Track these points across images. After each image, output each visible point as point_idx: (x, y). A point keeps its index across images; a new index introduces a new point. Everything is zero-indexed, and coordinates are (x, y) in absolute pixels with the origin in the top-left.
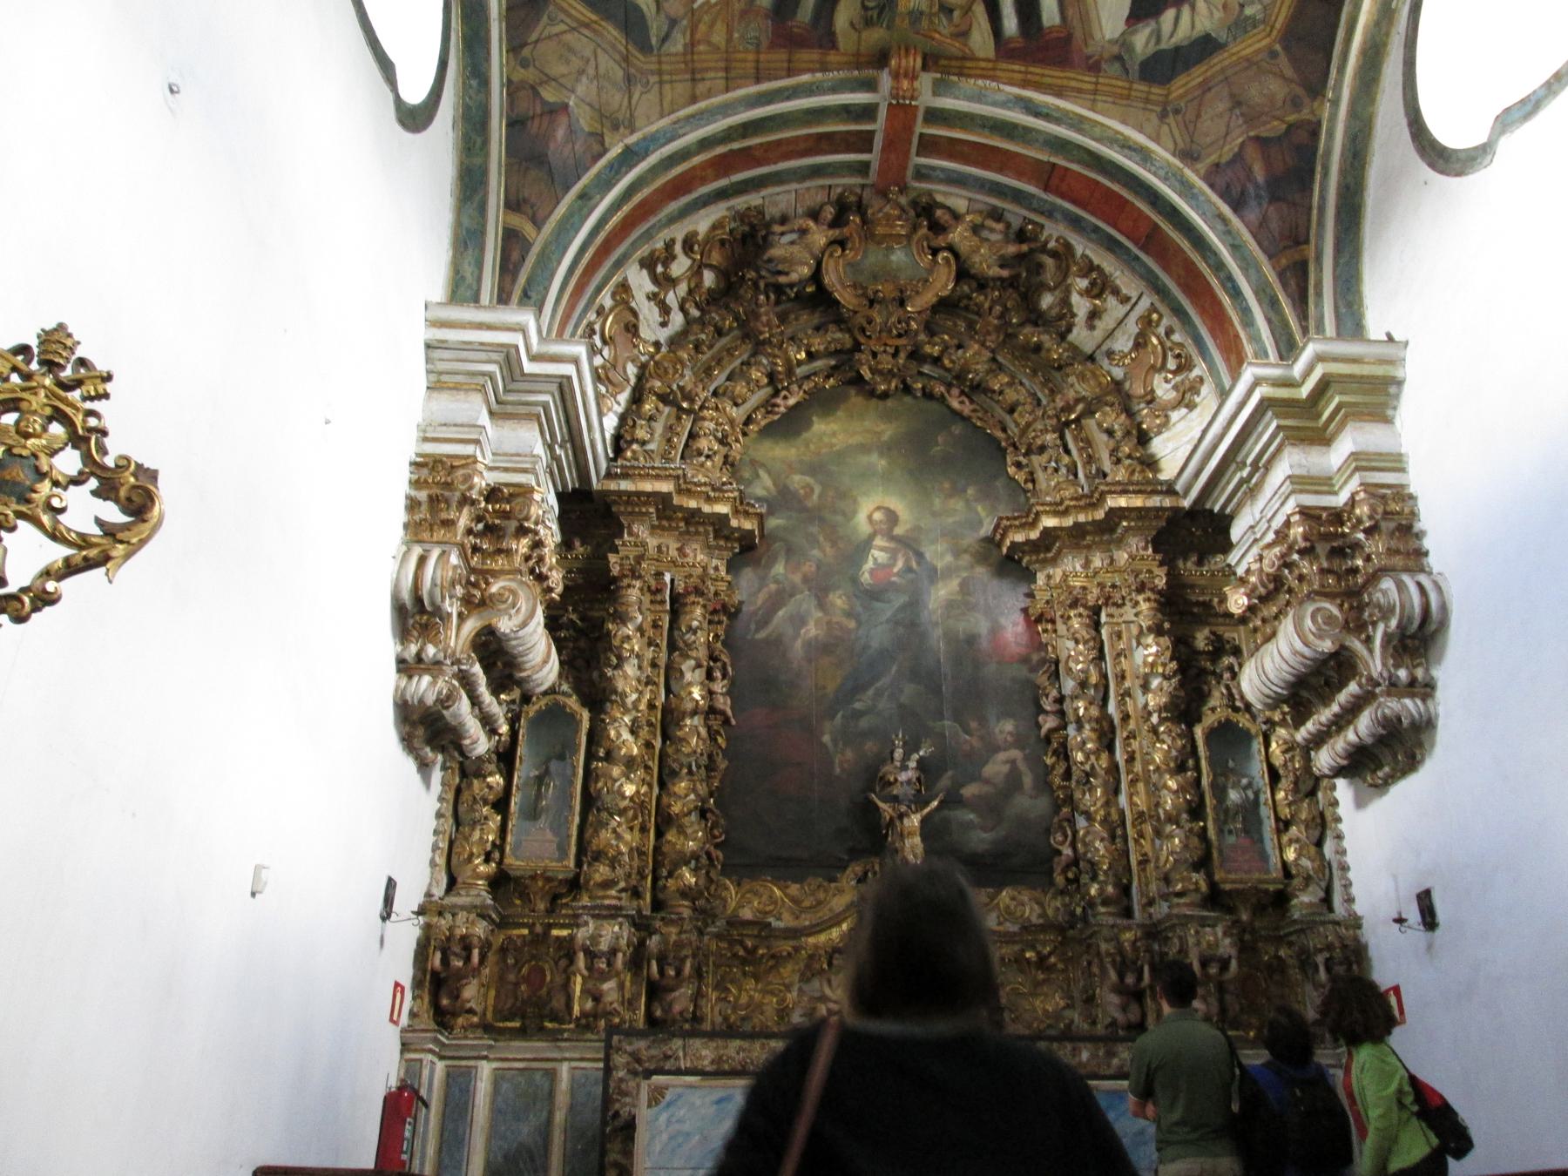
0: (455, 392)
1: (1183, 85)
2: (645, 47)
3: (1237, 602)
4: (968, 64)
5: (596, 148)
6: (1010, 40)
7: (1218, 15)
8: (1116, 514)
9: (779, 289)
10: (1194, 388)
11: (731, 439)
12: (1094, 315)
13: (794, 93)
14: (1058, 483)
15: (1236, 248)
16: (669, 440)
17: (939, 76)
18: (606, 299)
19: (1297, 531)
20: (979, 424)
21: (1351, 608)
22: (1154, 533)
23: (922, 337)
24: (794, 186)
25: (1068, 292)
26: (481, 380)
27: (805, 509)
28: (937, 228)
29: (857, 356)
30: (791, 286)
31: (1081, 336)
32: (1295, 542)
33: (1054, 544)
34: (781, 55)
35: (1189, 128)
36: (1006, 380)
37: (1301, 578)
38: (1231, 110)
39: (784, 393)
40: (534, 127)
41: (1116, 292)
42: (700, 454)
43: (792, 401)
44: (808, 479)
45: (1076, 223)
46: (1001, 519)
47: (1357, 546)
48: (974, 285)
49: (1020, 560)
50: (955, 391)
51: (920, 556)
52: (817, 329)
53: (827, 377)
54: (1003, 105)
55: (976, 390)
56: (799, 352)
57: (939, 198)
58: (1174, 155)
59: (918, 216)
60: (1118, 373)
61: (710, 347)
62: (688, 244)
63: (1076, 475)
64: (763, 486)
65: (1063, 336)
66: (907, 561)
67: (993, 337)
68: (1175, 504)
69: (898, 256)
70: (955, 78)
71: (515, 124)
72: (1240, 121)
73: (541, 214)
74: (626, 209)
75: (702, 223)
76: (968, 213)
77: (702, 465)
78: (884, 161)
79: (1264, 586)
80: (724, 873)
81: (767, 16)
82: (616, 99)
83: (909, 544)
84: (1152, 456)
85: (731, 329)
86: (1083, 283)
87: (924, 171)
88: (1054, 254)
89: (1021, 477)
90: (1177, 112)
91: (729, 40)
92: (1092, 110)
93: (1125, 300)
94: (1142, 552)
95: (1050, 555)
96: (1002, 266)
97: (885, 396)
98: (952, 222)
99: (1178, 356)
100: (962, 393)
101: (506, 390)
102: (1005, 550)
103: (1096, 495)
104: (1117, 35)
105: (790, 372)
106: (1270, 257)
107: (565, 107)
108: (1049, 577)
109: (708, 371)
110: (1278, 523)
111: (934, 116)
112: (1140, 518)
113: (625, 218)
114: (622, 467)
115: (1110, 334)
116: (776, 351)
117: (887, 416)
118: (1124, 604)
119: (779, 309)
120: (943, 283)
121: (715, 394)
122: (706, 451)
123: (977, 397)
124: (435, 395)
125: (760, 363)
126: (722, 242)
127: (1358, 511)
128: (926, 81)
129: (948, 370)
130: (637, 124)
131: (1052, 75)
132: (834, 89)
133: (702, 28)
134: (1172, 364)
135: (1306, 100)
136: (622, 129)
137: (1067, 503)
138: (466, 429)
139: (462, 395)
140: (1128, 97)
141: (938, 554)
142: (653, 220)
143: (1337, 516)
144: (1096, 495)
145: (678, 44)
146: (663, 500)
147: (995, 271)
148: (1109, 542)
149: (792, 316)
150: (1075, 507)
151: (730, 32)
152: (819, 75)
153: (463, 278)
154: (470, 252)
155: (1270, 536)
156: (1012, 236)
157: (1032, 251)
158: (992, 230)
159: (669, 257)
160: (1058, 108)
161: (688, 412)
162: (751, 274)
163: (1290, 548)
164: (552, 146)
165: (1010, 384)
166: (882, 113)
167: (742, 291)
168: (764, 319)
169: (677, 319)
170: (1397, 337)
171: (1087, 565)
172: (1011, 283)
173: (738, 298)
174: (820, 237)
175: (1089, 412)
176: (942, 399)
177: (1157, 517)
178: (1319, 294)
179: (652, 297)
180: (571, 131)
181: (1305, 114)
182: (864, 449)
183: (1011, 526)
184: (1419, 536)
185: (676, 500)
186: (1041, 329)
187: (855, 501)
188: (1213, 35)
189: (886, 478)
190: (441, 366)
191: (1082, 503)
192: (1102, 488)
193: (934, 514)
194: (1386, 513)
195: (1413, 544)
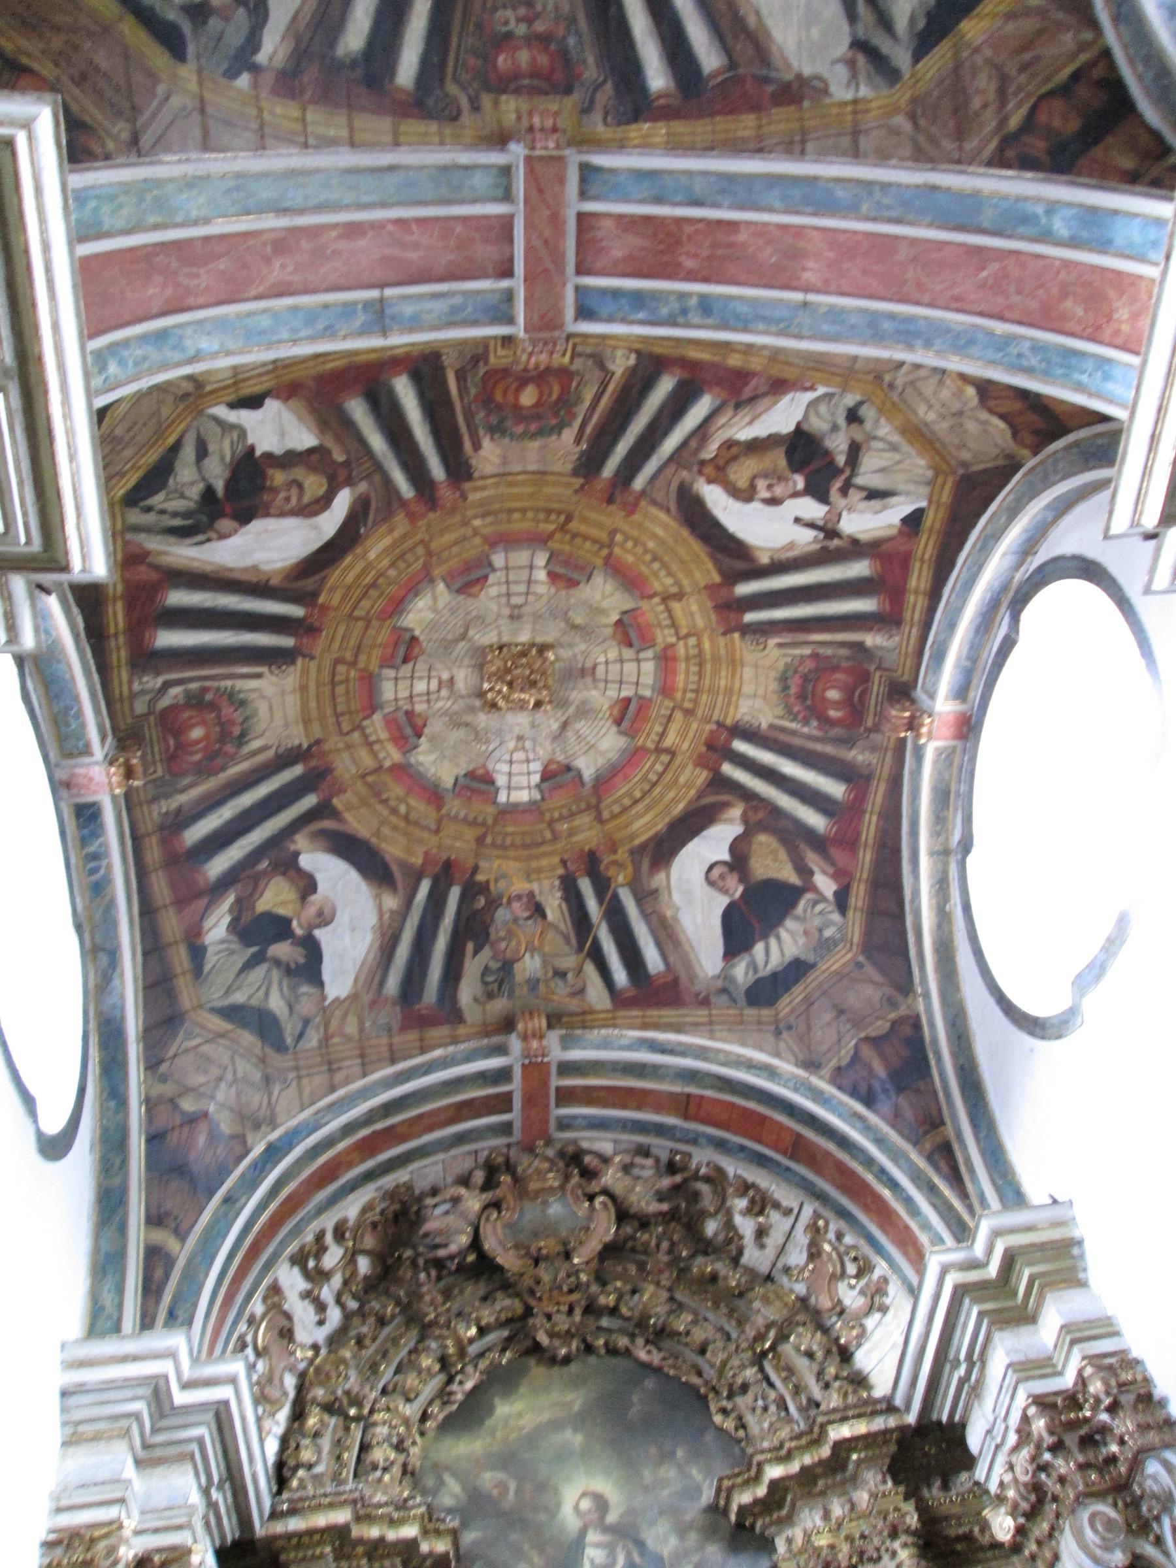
0: (94, 1444)
1: (788, 1004)
2: (280, 1047)
3: (1003, 1526)
4: (589, 1017)
5: (239, 1149)
6: (622, 991)
7: (802, 940)
8: (843, 1447)
9: (439, 1264)
10: (880, 1289)
11: (408, 1443)
12: (761, 1233)
13: (429, 1068)
14: (771, 1425)
15: (880, 1141)
16: (339, 1457)
17: (564, 1032)
18: (257, 1306)
19: (1039, 1425)
20: (672, 1372)
21: (1126, 1505)
22: (887, 1461)
23: (594, 1288)
24: (440, 1156)
25: (729, 1214)
26: (124, 1423)
27: (501, 1514)
28: (588, 1174)
29: (531, 1321)
30: (451, 1257)
31: (753, 1257)
32: (1041, 1439)
33: (784, 1499)
34: (412, 1036)
35: (805, 1040)
36: (690, 1318)
37: (1062, 1480)
38: (837, 1017)
39: (458, 1378)
40: (173, 1139)
41: (777, 1205)
42: (375, 1467)
43: (469, 1385)
44: (500, 1475)
45: (721, 1145)
46: (721, 1480)
47: (1104, 1429)
48: (636, 1223)
49: (753, 1527)
50: (640, 1341)
51: (641, 1545)
52: (484, 1299)
53: (503, 1350)
54: (629, 1048)
55: (660, 1335)
56: (468, 1328)
57: (585, 1145)
58: (797, 1065)
59: (568, 1165)
60: (800, 1289)
61: (374, 1339)
62: (339, 1233)
63: (786, 1409)
64: (452, 1493)
65: (736, 1261)
66: (629, 1554)
67: (666, 1274)
68: (899, 1423)
69: (555, 1209)
70: (579, 1032)
71: (154, 1139)
72: (849, 1026)
73: (185, 1226)
74: (273, 1206)
75: (351, 1209)
76: (615, 1154)
77: (380, 1480)
78: (526, 1119)
79: (1026, 1499)
81: (394, 1004)
82: (256, 1099)
84: (859, 1373)
85: (393, 1316)
86: (742, 1203)
87: (565, 1121)
88: (707, 1180)
89: (729, 1424)
90: (789, 1028)
91: (361, 1030)
92: (712, 1038)
93: (788, 1212)
94: (882, 1488)
95: (784, 1512)
96: (661, 1200)
97: (567, 1360)
98: (602, 1166)
99: (855, 1259)
100: (647, 1342)
101: (155, 1430)
102: (733, 1517)
103: (816, 1429)
104: (718, 971)
105: (462, 1352)
106: (915, 1143)
107: (205, 1115)
108: (789, 1541)
109: (374, 1367)
110: (1015, 1419)
111: (566, 1068)
112: (867, 1447)
113: (272, 1217)
114: (290, 1501)
115: (782, 1250)
116: (445, 1332)
117: (575, 1383)
118: (879, 1558)
119: (441, 1284)
120: (605, 1229)
121: (384, 1392)
122: (381, 1464)
123: (666, 1343)
124: (71, 1450)
125: (427, 1349)
126: (374, 1225)
127: (1092, 1389)
128: (553, 1039)
129: (628, 1319)
130: (279, 1121)
131: (668, 1014)
132: (468, 1059)
133: (334, 1023)
134: (851, 1269)
135: (900, 998)
136: (263, 1128)
137: (787, 1445)
138: (108, 1487)
139: (102, 1445)
140: (742, 1023)
142: (301, 1214)
143: (1073, 1400)
144: (816, 1429)
145: (313, 1039)
146: (339, 1534)
147: (654, 1207)
148: (844, 1482)
149: (456, 1291)
150: (798, 1448)
151: (361, 1023)
152: (451, 1049)
153: (102, 1308)
154: (109, 1277)
155: (1012, 1438)
156: (663, 1169)
157: (685, 1181)
158: (643, 1167)
159: (320, 1248)
160: (680, 1044)
161: (357, 1419)
162: (408, 1253)
163: (1038, 1447)
164: (193, 1156)
165: (695, 1322)
166: (517, 1073)
167: (401, 1273)
168: (427, 1298)
169: (334, 1316)
170: (1060, 1199)
171: (826, 1516)
172: (671, 1216)
173: (397, 1281)
174: (473, 1203)
175: (783, 1337)
176: (627, 1353)
177: (886, 1442)
178: (971, 1170)
179: (306, 1295)
180: (213, 1137)
181: (903, 1011)
182: (556, 1425)
183: (733, 1486)
184: (1162, 1403)
185: (356, 1532)
186: (712, 1257)
187: (556, 1492)
188: (803, 957)
189: (586, 1454)
190: (78, 1415)
191: (803, 1441)
192: (820, 1419)
193: (646, 1489)
194: (1121, 1385)
195: (1160, 1416)
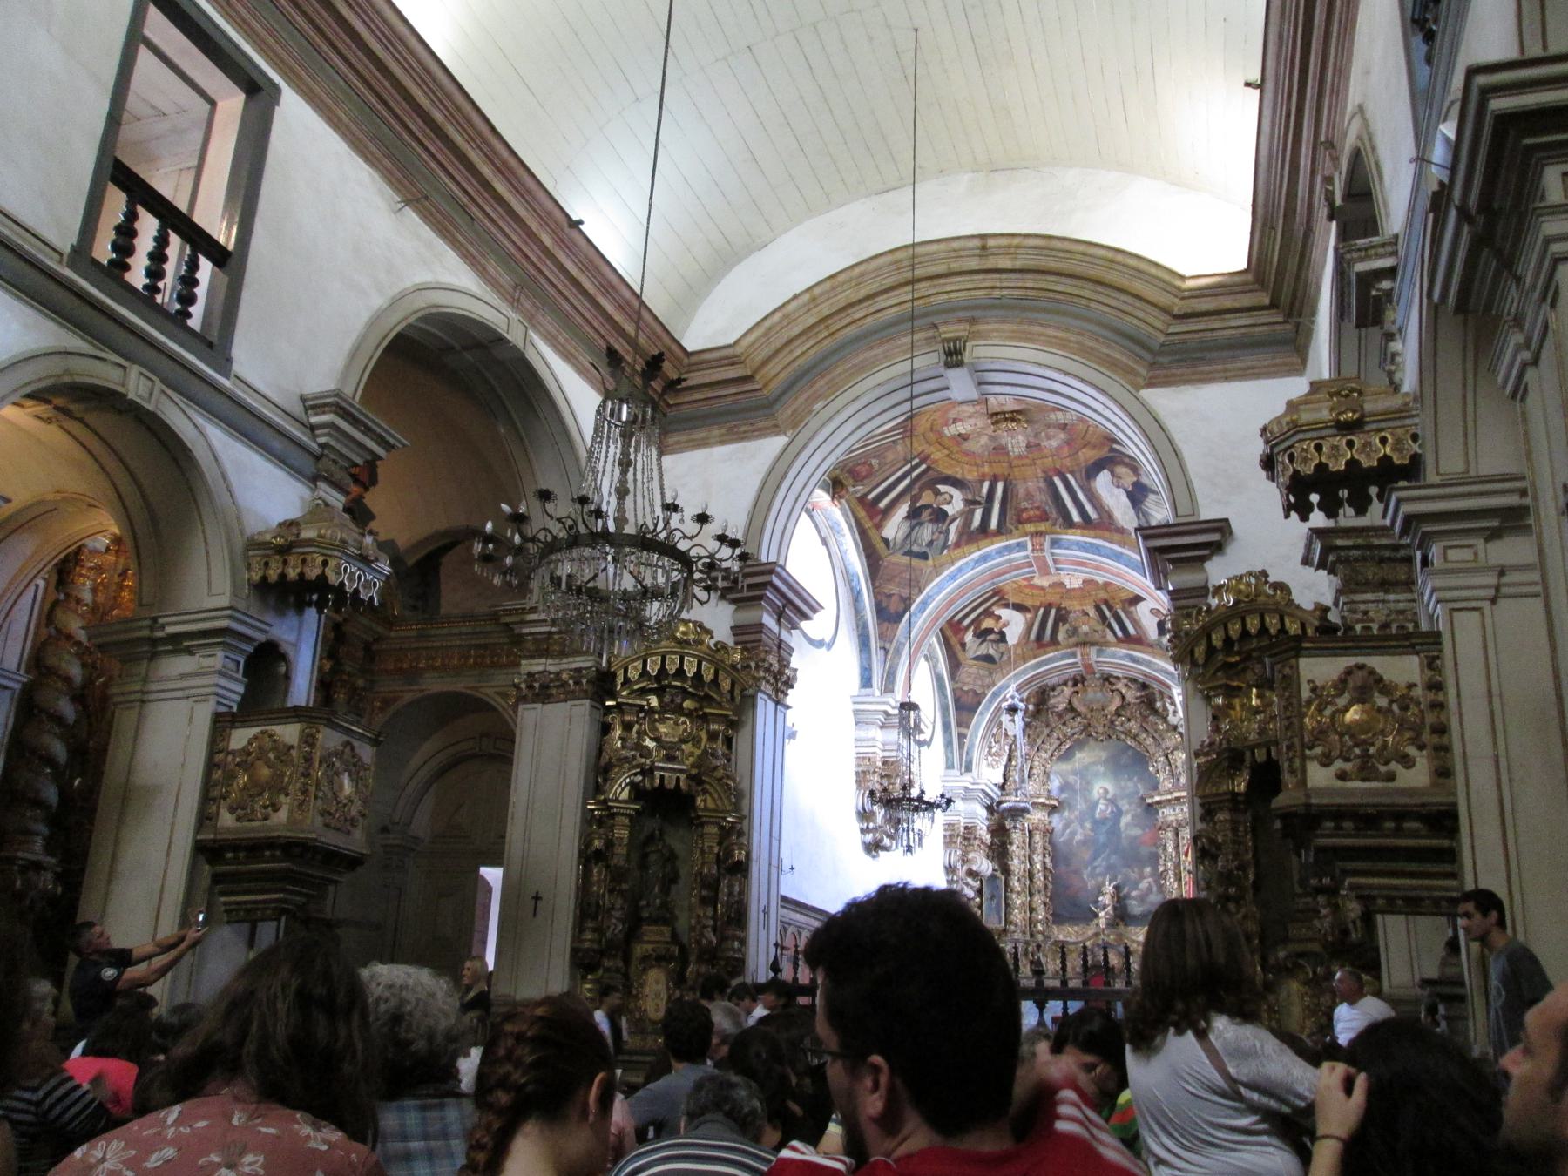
80: (1054, 922)
83: (1112, 802)
117: (1104, 749)
141: (1124, 805)
182: (1094, 763)
189: (1104, 775)
